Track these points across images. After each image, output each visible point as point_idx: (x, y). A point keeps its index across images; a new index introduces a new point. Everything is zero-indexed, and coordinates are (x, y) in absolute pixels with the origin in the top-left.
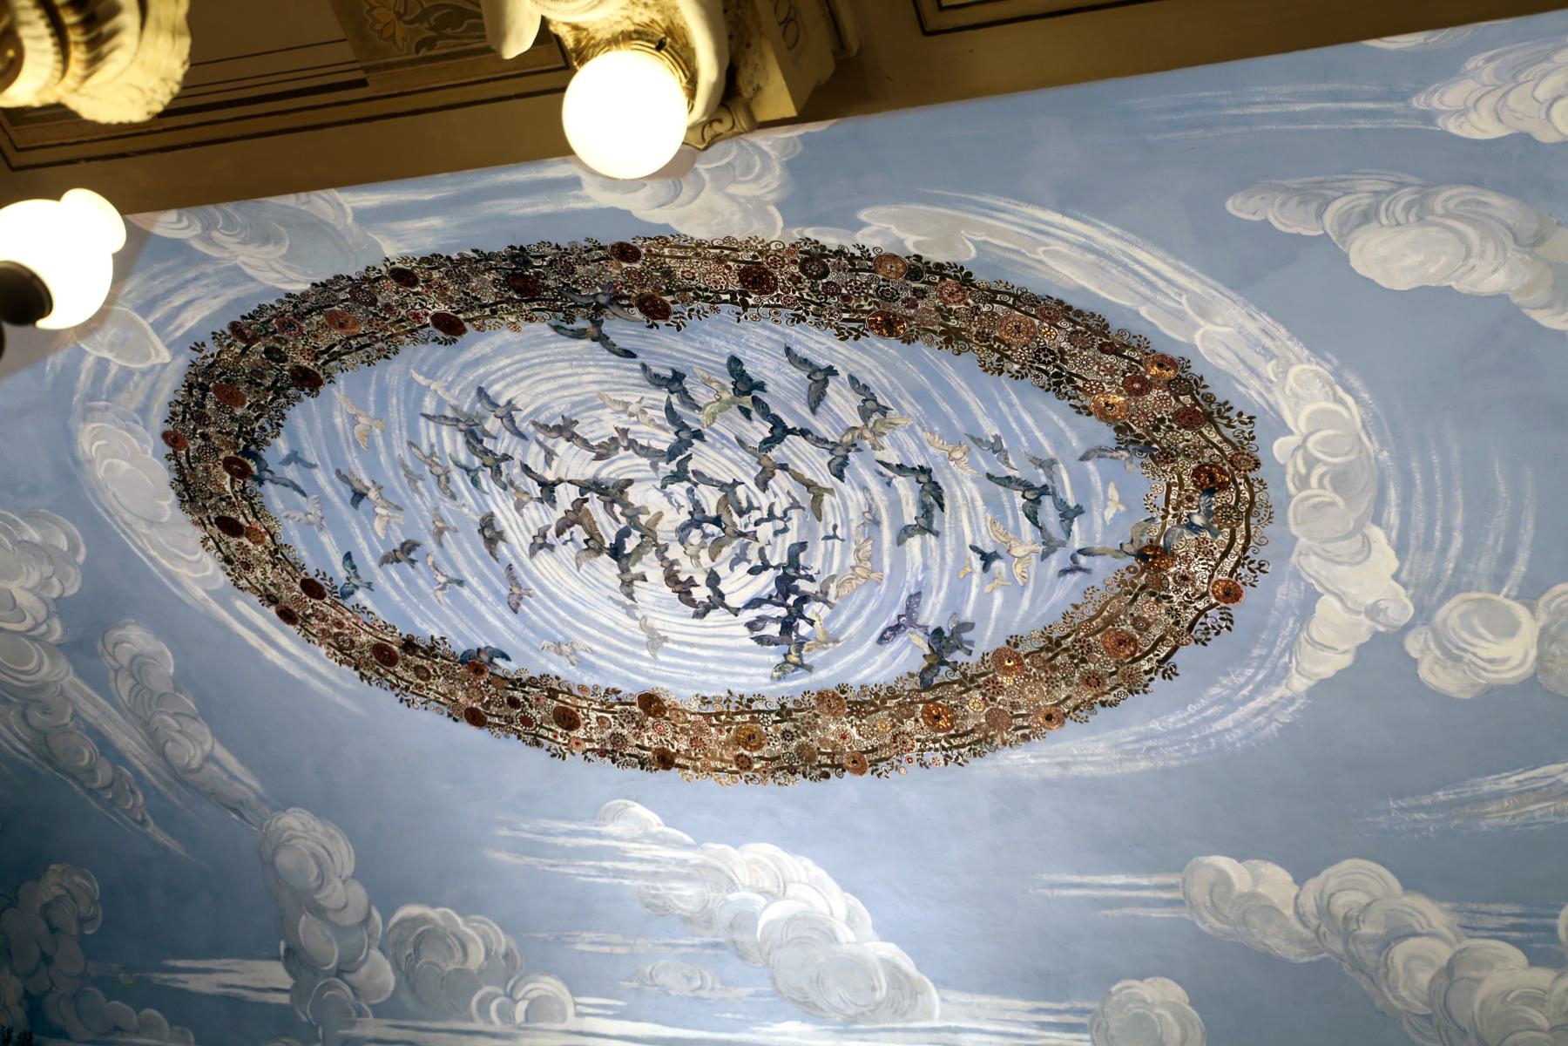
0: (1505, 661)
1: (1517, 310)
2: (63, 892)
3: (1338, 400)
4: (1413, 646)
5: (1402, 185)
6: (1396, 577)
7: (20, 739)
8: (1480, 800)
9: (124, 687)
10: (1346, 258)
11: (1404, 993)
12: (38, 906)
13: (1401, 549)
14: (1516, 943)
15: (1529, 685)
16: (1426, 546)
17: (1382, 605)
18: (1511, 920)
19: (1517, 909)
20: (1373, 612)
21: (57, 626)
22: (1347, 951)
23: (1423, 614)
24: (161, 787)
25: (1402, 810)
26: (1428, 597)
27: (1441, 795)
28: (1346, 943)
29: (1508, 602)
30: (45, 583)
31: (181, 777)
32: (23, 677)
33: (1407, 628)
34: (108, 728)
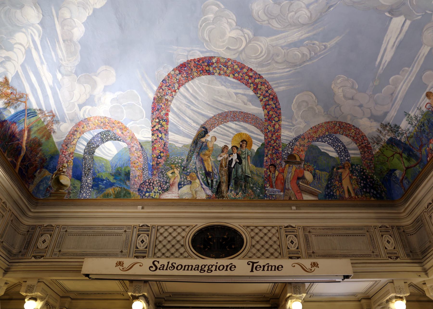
2: (342, 88)
7: (284, 69)
9: (275, 24)
12: (343, 99)
21: (246, 31)
24: (314, 32)
30: (230, 24)
31: (313, 22)
32: (263, 54)
34: (290, 40)
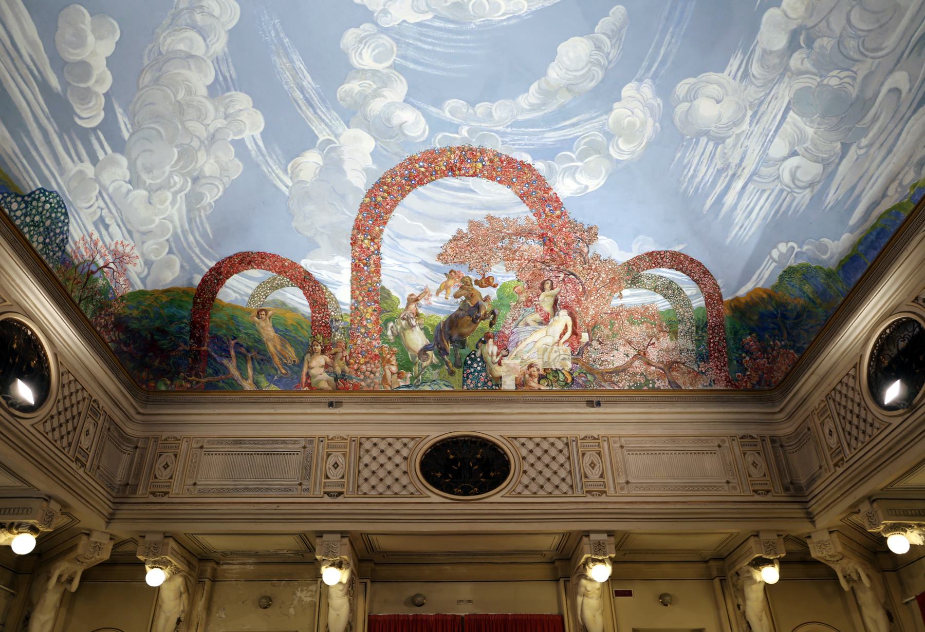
0: (361, 58)
1: (539, 78)
3: (503, 15)
4: (367, 26)
5: (610, 62)
6: (404, 21)
8: (287, 55)
10: (581, 36)
11: (169, 40)
13: (419, 24)
14: (216, 79)
15: (351, 67)
16: (421, 34)
17: (389, 16)
18: (228, 75)
19: (234, 76)
20: (385, 12)
22: (182, 10)
23: (385, 31)
25: (274, 25)
26: (397, 33)
27: (286, 40)
28: (187, 9)
29: (392, 60)
33: (377, 25)
